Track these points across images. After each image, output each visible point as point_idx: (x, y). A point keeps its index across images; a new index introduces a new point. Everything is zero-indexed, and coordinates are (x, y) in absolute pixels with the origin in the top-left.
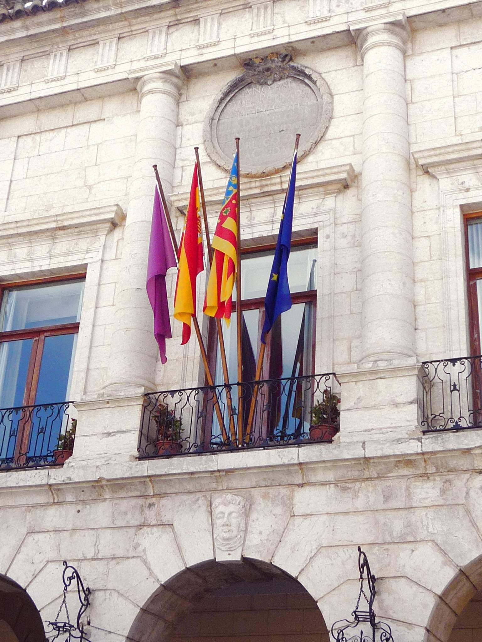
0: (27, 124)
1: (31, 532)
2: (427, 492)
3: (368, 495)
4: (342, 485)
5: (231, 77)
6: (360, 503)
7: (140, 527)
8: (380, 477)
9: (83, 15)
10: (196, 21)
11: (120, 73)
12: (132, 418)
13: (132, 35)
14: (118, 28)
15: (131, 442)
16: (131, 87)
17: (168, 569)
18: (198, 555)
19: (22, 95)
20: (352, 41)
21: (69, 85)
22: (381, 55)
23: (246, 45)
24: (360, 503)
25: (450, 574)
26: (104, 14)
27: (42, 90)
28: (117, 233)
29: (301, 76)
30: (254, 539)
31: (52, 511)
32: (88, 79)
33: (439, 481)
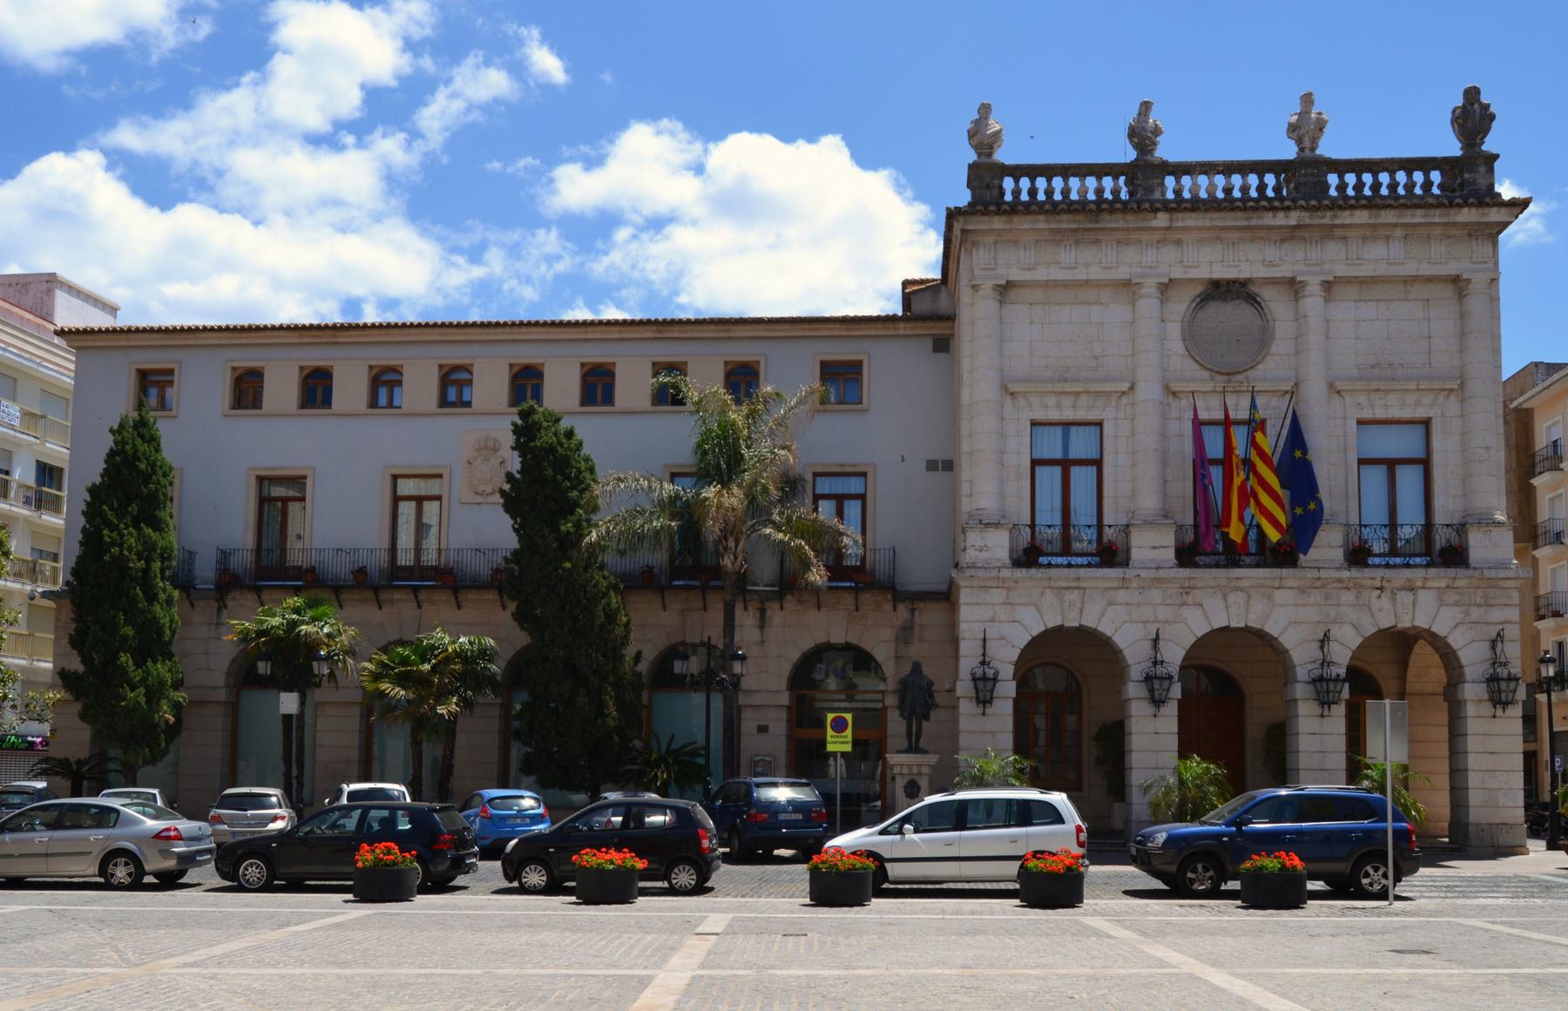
0: (1037, 294)
1: (1110, 604)
2: (1348, 597)
3: (1316, 597)
4: (1302, 590)
5: (1199, 289)
6: (1312, 600)
7: (1183, 604)
8: (1323, 586)
9: (1097, 222)
10: (1179, 243)
11: (1122, 273)
12: (1168, 538)
13: (1128, 243)
14: (1118, 235)
15: (1170, 555)
16: (1128, 286)
17: (1202, 629)
18: (1219, 622)
19: (1041, 274)
20: (1293, 286)
21: (1080, 274)
22: (1313, 302)
23: (1220, 273)
24: (1312, 600)
25: (1359, 640)
26: (1113, 225)
27: (1056, 274)
28: (1124, 400)
29: (1253, 300)
30: (1252, 616)
31: (1122, 593)
32: (1096, 273)
33: (1354, 592)
